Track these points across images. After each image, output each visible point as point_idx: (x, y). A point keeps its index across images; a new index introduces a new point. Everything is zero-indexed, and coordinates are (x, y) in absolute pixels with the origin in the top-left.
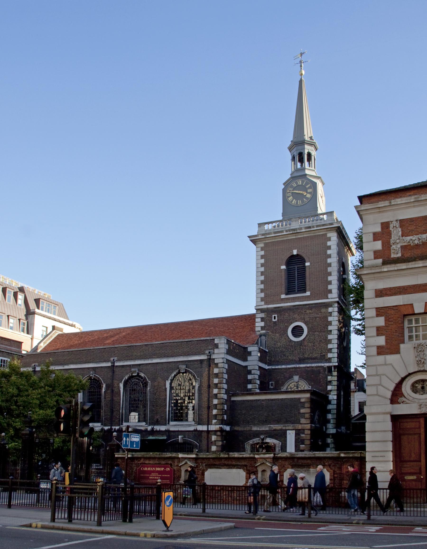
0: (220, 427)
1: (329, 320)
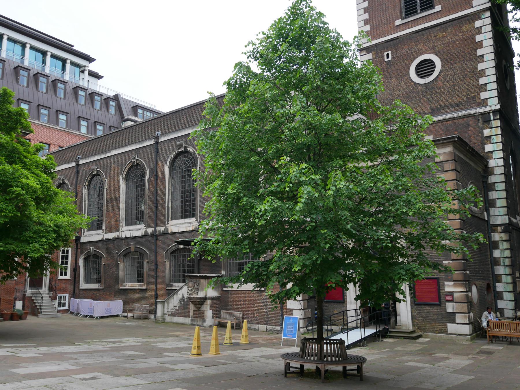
1: (477, 40)
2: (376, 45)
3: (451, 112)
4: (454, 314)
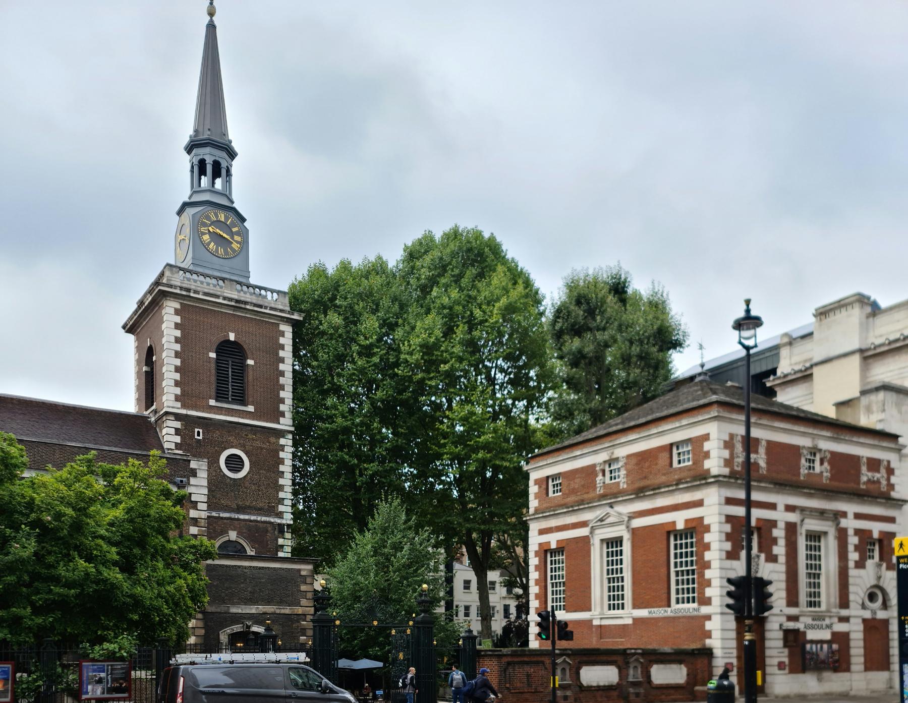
2: (187, 415)
3: (254, 515)
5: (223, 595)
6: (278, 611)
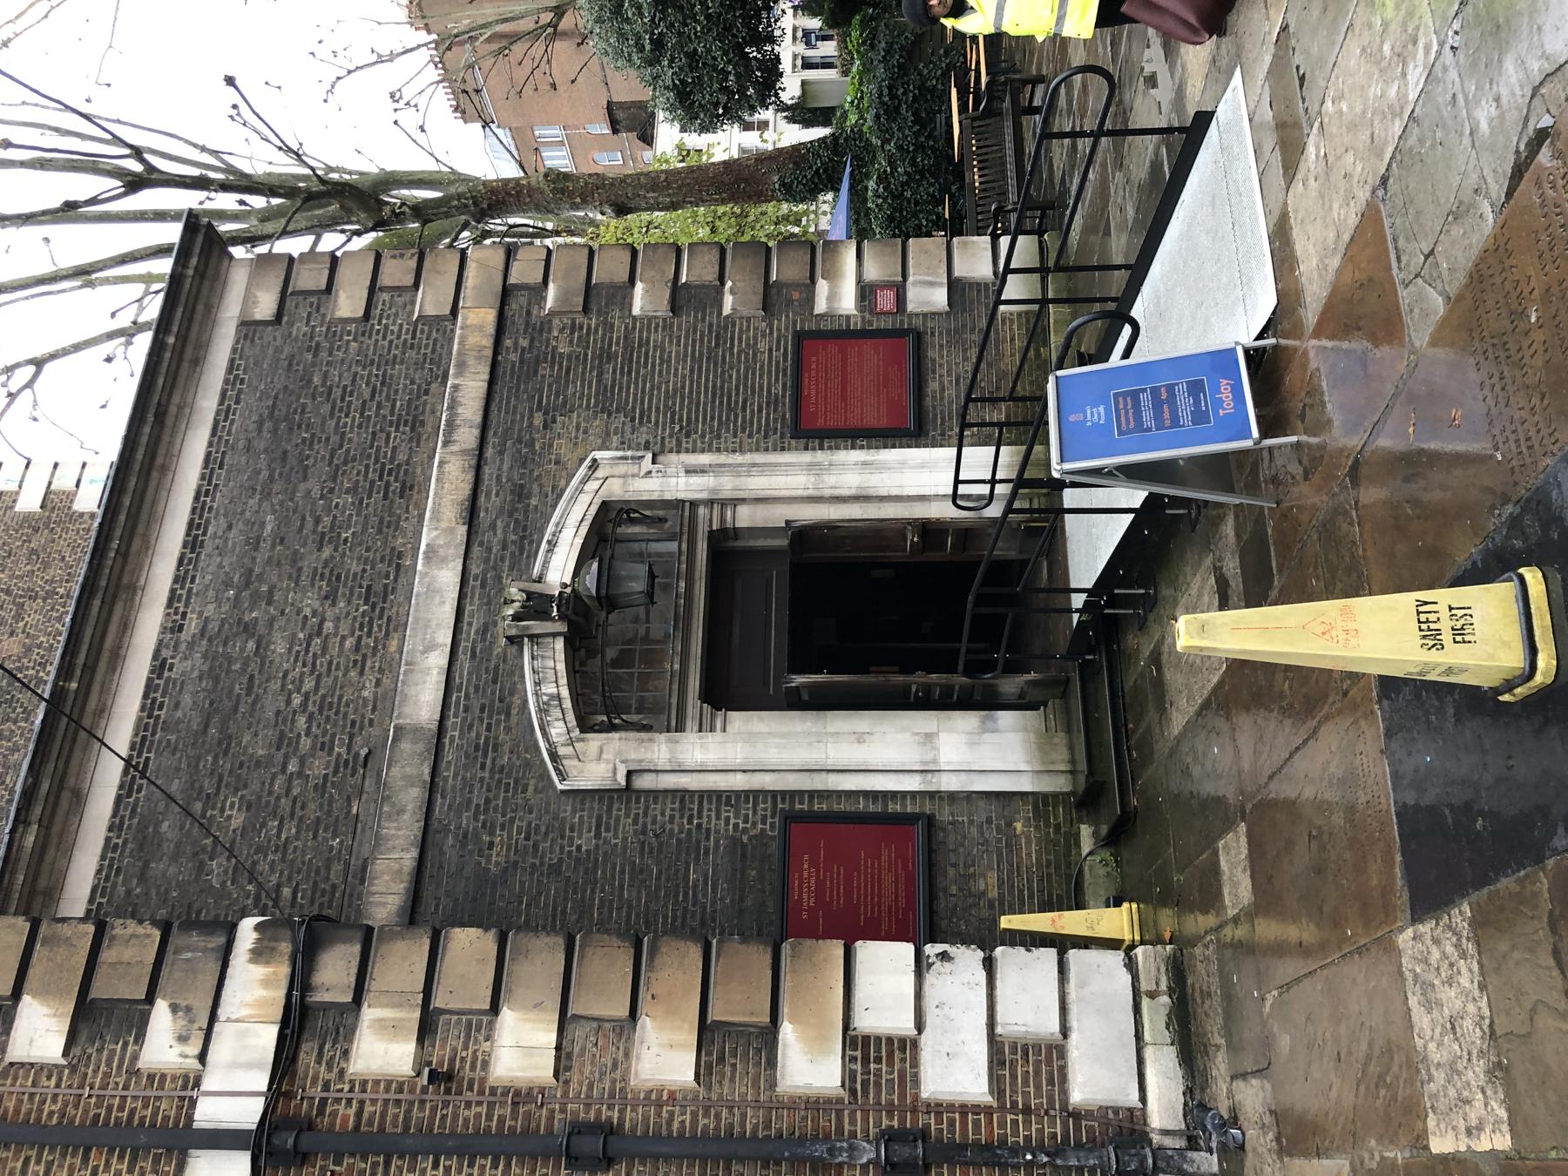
0: (258, 955)
4: (956, 287)
5: (318, 767)
6: (467, 436)
